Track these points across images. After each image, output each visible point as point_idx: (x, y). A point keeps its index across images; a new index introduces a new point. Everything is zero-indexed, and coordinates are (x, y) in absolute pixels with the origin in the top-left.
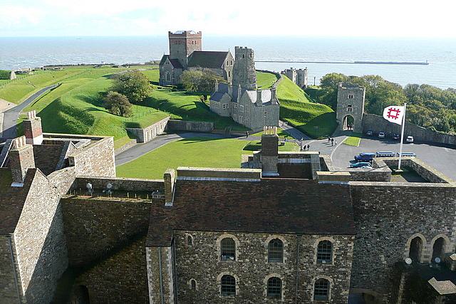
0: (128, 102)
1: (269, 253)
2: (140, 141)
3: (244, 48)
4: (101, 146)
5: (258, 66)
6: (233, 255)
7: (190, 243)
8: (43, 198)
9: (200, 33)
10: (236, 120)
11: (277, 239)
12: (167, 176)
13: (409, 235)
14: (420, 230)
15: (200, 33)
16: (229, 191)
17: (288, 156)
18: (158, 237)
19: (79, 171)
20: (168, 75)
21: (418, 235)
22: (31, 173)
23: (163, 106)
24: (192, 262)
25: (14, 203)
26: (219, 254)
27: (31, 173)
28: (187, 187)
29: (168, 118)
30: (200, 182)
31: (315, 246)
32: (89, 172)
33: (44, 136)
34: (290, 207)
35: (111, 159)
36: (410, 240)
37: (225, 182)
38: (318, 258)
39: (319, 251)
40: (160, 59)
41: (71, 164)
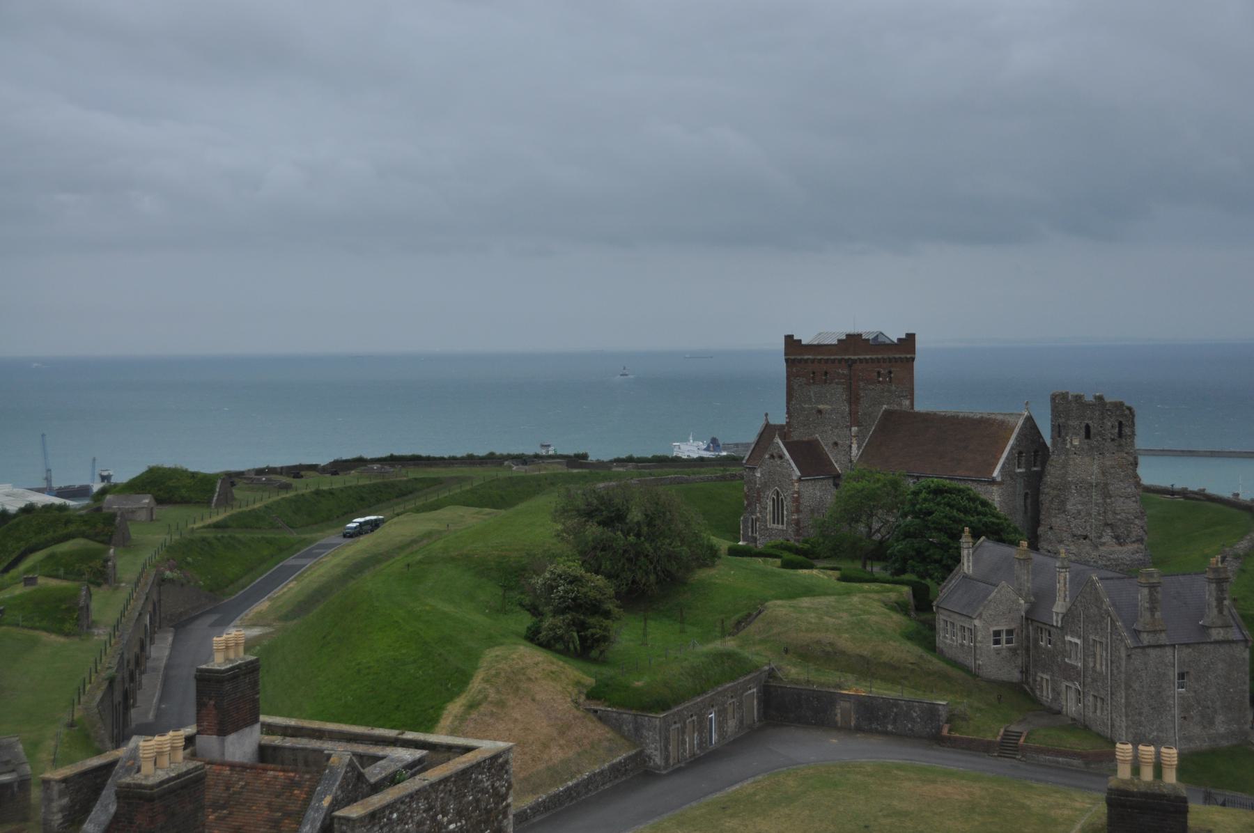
3: (1089, 398)
5: (1152, 473)
9: (911, 338)
10: (1046, 695)
15: (911, 338)
20: (778, 503)
40: (752, 438)
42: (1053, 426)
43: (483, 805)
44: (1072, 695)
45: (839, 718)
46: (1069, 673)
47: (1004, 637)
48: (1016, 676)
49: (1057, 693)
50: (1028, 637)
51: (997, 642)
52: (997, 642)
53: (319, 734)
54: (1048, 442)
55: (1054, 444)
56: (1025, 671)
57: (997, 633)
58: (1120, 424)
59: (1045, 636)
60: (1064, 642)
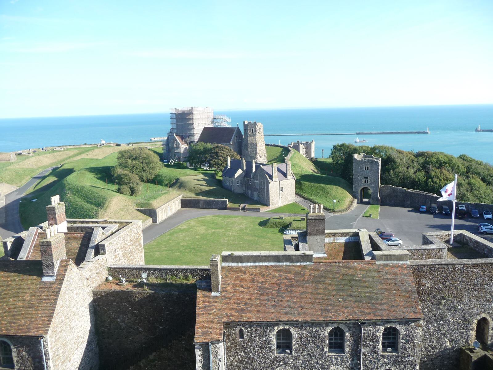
0: (138, 181)
1: (329, 343)
2: (155, 221)
4: (131, 230)
6: (290, 347)
7: (242, 336)
8: (75, 292)
10: (250, 195)
11: (338, 327)
12: (214, 264)
13: (473, 315)
14: (485, 310)
16: (281, 276)
17: (334, 235)
18: (207, 331)
19: (110, 259)
21: (483, 315)
22: (64, 266)
23: (176, 184)
24: (243, 357)
25: (45, 300)
26: (274, 347)
27: (64, 266)
28: (233, 275)
29: (180, 197)
30: (246, 267)
31: (380, 334)
32: (120, 260)
33: (68, 222)
34: (349, 291)
35: (140, 244)
36: (476, 321)
37: (276, 266)
38: (383, 346)
39: (383, 338)
41: (101, 252)
42: (244, 130)
43: (136, 237)
44: (256, 195)
45: (201, 206)
46: (256, 190)
47: (239, 182)
48: (242, 191)
49: (253, 194)
50: (245, 182)
51: (238, 184)
52: (238, 184)
53: (88, 222)
54: (243, 134)
55: (244, 134)
56: (245, 190)
57: (238, 182)
58: (260, 129)
59: (249, 181)
60: (254, 182)
